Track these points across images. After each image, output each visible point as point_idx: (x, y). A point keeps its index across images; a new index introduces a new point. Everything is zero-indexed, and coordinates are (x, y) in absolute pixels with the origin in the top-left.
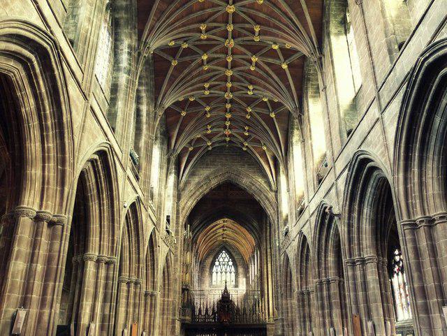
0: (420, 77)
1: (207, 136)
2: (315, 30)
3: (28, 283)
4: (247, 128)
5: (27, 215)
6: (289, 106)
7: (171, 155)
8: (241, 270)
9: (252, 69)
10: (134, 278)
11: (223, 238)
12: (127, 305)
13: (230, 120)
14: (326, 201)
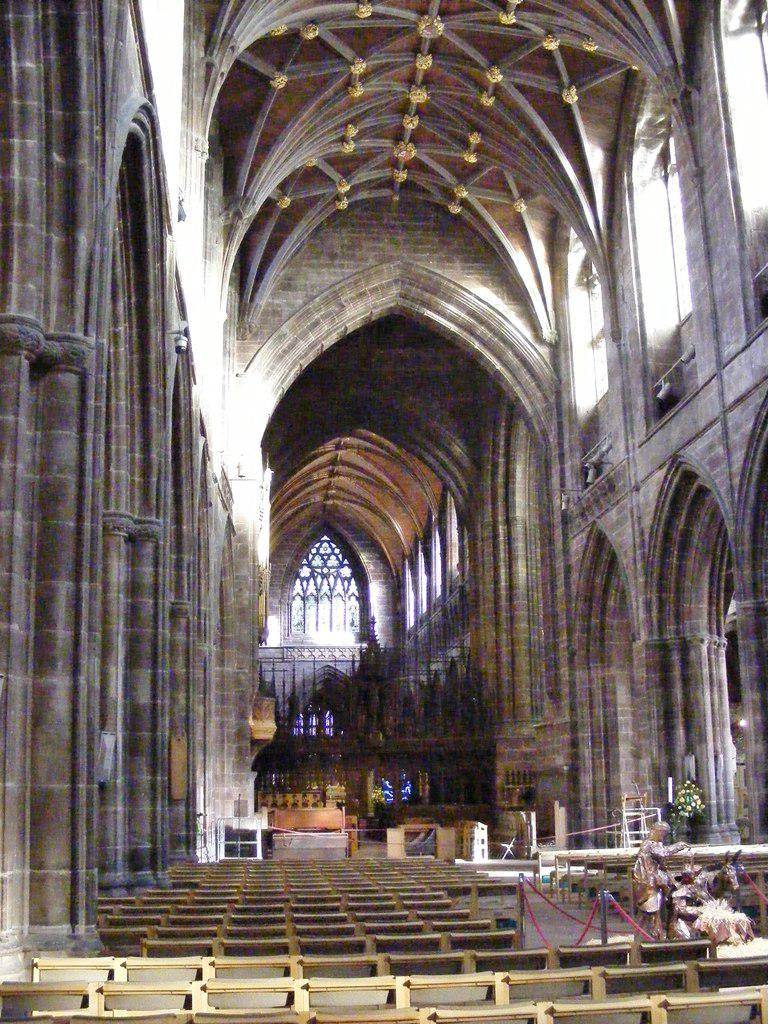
4: (475, 139)
11: (327, 497)
13: (420, 111)
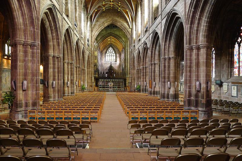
0: (171, 15)
1: (102, 5)
3: (54, 75)
5: (51, 56)
8: (118, 55)
10: (78, 66)
12: (77, 74)
14: (146, 41)
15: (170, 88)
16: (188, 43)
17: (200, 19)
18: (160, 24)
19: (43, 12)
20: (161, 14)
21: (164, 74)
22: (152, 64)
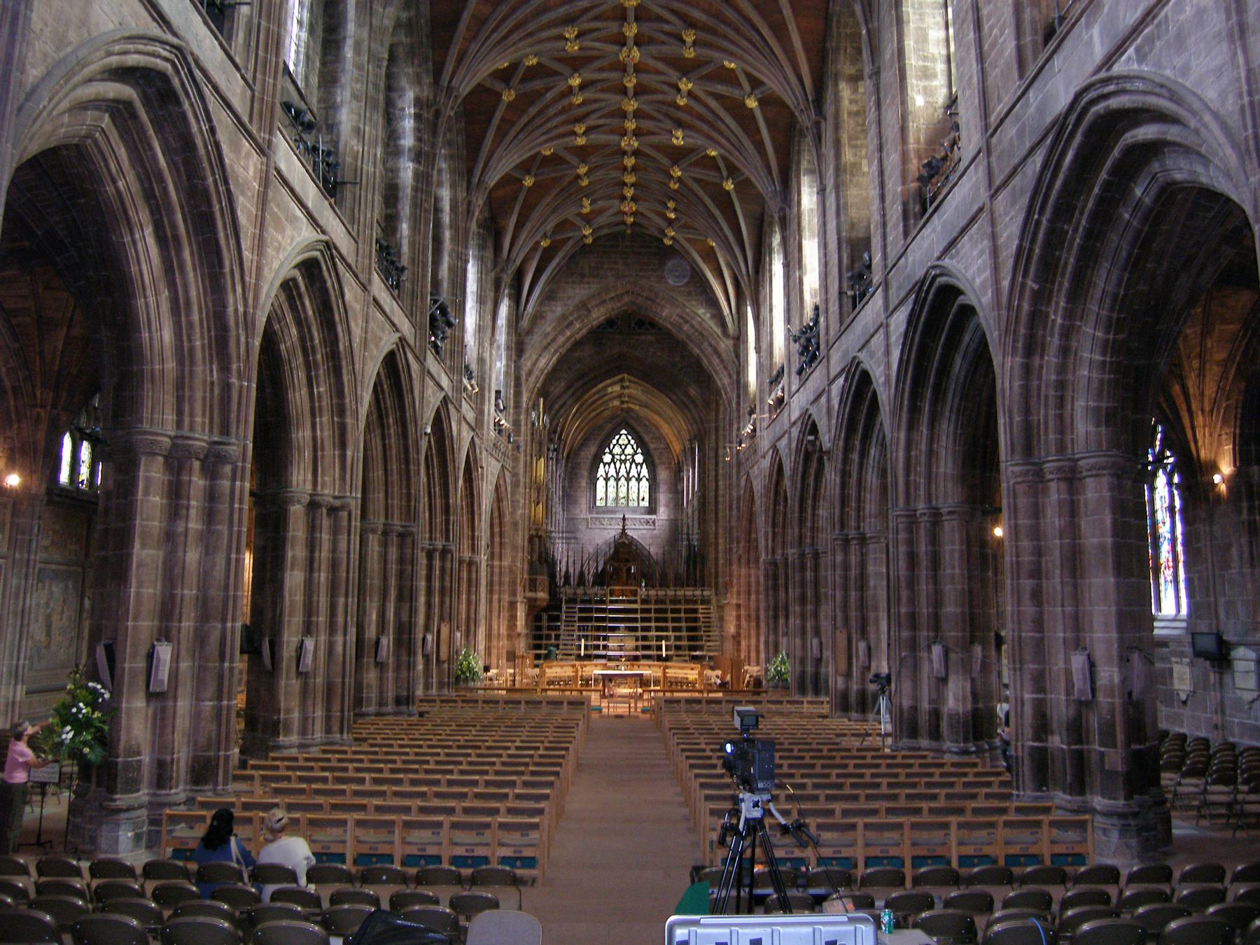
1: (579, 215)
2: (809, 61)
5: (299, 502)
6: (764, 186)
7: (503, 270)
8: (663, 475)
9: (681, 102)
10: (439, 544)
11: (623, 402)
13: (633, 185)
14: (813, 410)
15: (944, 680)
16: (1018, 449)
17: (1067, 333)
18: (880, 337)
19: (278, 283)
20: (886, 284)
21: (912, 600)
22: (846, 542)
